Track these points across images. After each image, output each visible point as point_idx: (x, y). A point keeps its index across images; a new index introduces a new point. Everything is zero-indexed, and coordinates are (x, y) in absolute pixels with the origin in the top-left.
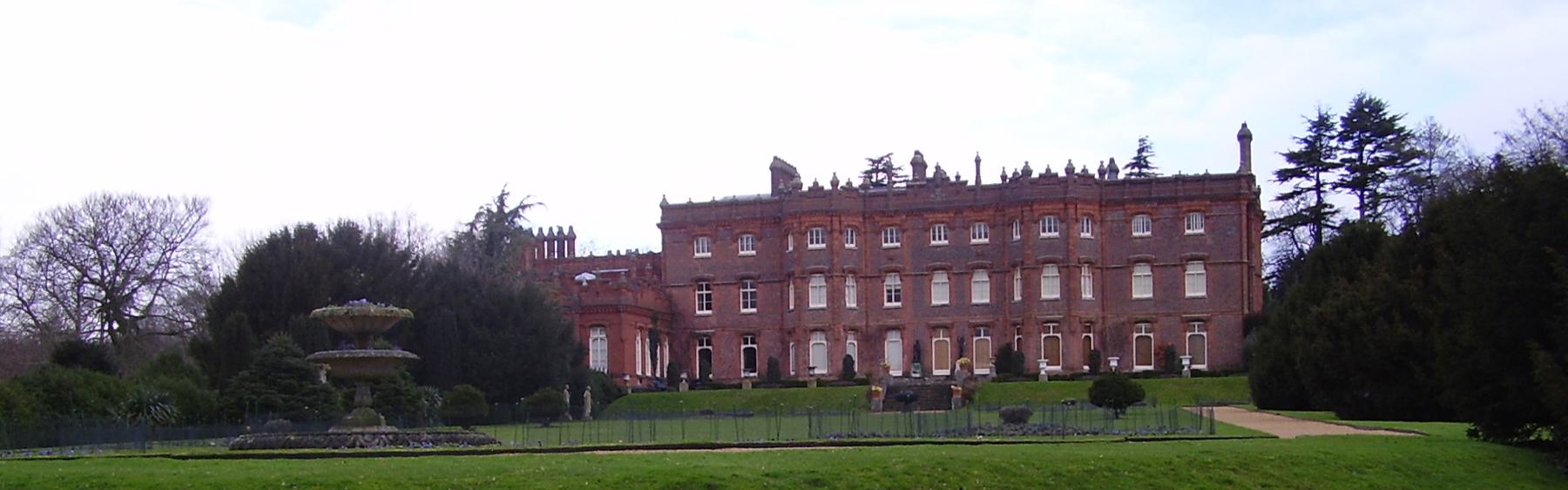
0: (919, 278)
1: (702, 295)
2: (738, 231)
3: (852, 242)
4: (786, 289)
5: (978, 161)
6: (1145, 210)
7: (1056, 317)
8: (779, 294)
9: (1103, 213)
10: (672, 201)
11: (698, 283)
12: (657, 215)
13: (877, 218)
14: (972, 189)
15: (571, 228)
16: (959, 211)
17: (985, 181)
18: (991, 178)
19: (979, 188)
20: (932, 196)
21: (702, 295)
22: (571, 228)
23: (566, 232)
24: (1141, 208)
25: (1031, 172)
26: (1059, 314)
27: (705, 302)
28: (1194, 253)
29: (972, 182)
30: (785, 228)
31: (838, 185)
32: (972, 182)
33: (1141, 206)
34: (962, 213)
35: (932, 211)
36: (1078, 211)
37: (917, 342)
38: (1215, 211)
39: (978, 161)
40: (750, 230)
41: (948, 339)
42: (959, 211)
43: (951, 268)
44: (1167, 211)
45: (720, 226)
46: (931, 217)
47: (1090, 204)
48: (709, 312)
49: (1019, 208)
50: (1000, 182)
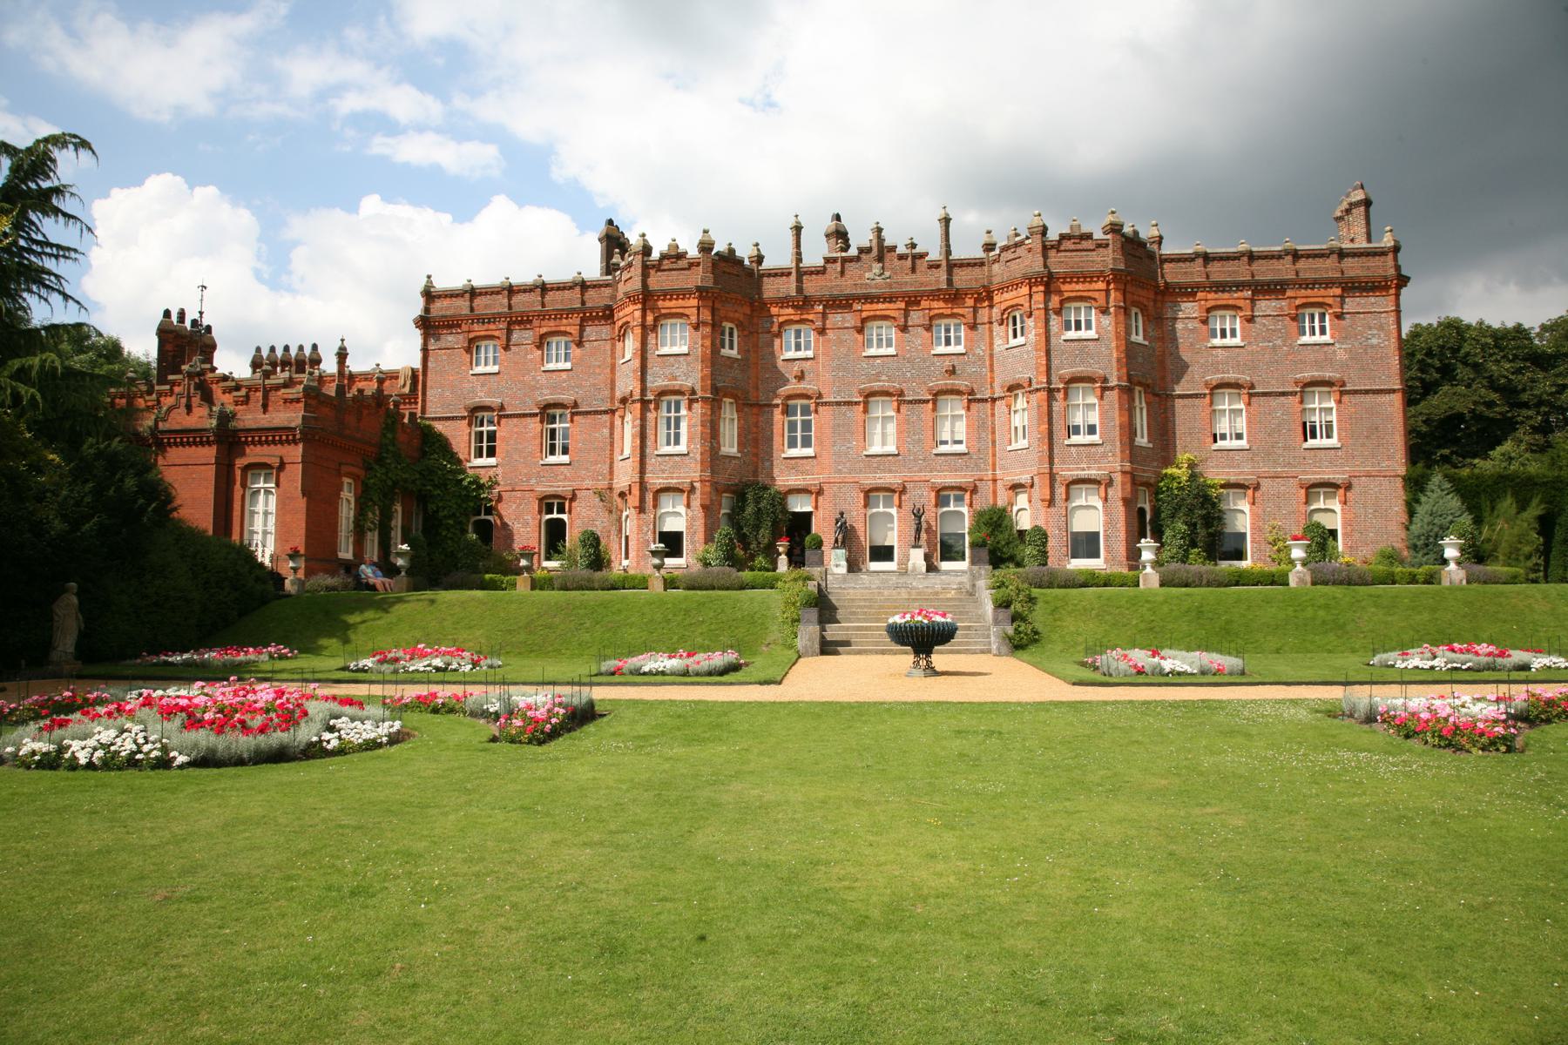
0: (844, 408)
1: (482, 433)
2: (544, 330)
3: (731, 348)
4: (618, 422)
5: (946, 221)
6: (1230, 302)
7: (1093, 473)
8: (606, 431)
9: (1159, 305)
10: (440, 284)
11: (475, 413)
12: (417, 307)
13: (774, 310)
14: (934, 266)
15: (315, 347)
16: (912, 300)
17: (957, 254)
18: (966, 247)
19: (952, 266)
20: (867, 275)
21: (482, 433)
22: (315, 347)
23: (308, 351)
24: (1224, 297)
25: (1044, 230)
26: (1099, 469)
27: (485, 445)
28: (1316, 374)
29: (935, 254)
30: (620, 323)
31: (712, 249)
32: (935, 254)
33: (1226, 295)
34: (918, 303)
35: (869, 298)
36: (1128, 295)
37: (842, 514)
38: (1351, 304)
39: (946, 221)
40: (563, 329)
41: (894, 511)
42: (912, 300)
43: (901, 394)
44: (1266, 306)
45: (515, 322)
46: (869, 309)
47: (1143, 288)
48: (492, 461)
49: (1025, 290)
50: (979, 253)
